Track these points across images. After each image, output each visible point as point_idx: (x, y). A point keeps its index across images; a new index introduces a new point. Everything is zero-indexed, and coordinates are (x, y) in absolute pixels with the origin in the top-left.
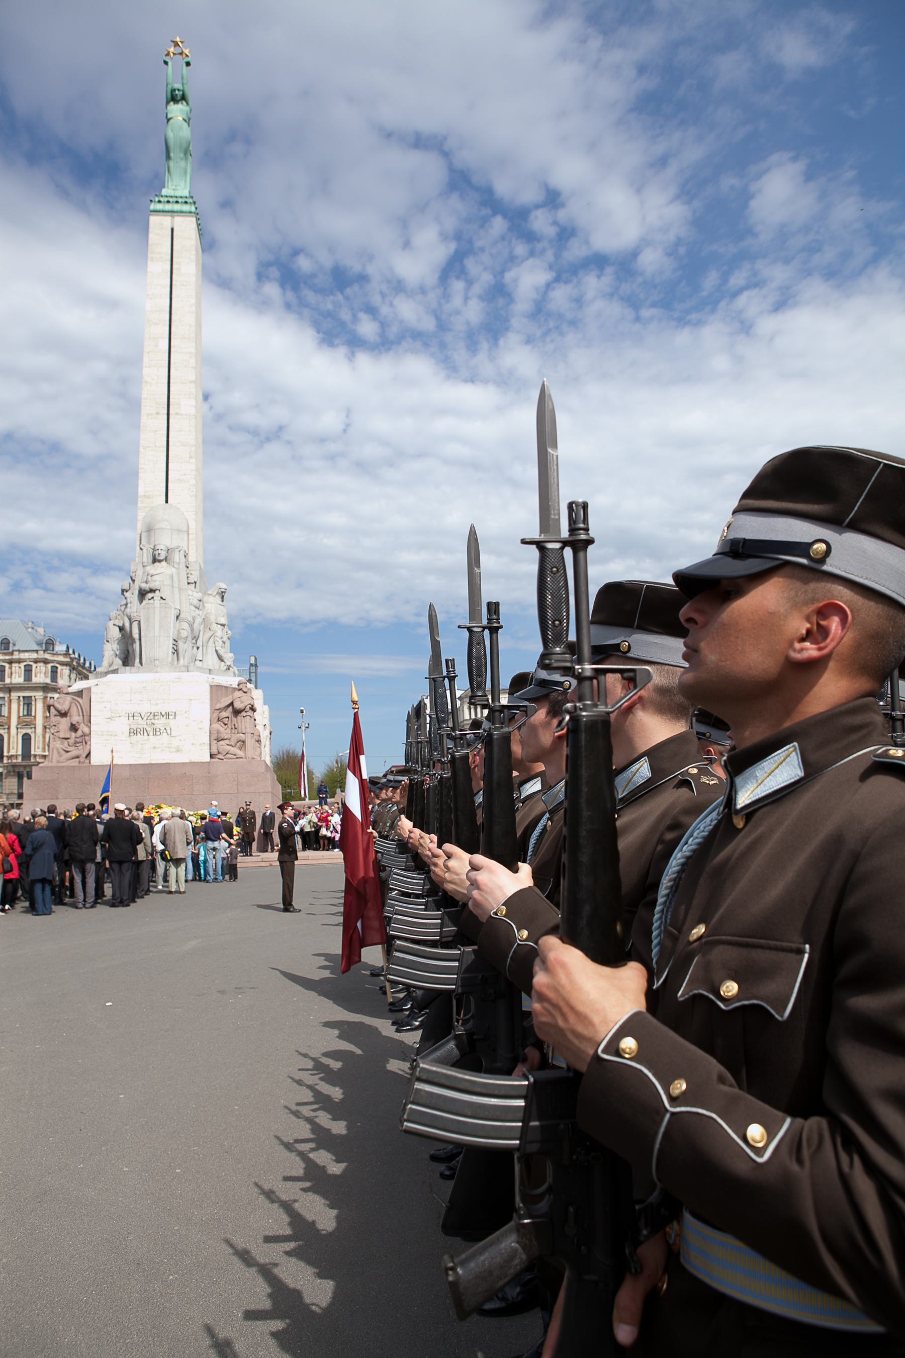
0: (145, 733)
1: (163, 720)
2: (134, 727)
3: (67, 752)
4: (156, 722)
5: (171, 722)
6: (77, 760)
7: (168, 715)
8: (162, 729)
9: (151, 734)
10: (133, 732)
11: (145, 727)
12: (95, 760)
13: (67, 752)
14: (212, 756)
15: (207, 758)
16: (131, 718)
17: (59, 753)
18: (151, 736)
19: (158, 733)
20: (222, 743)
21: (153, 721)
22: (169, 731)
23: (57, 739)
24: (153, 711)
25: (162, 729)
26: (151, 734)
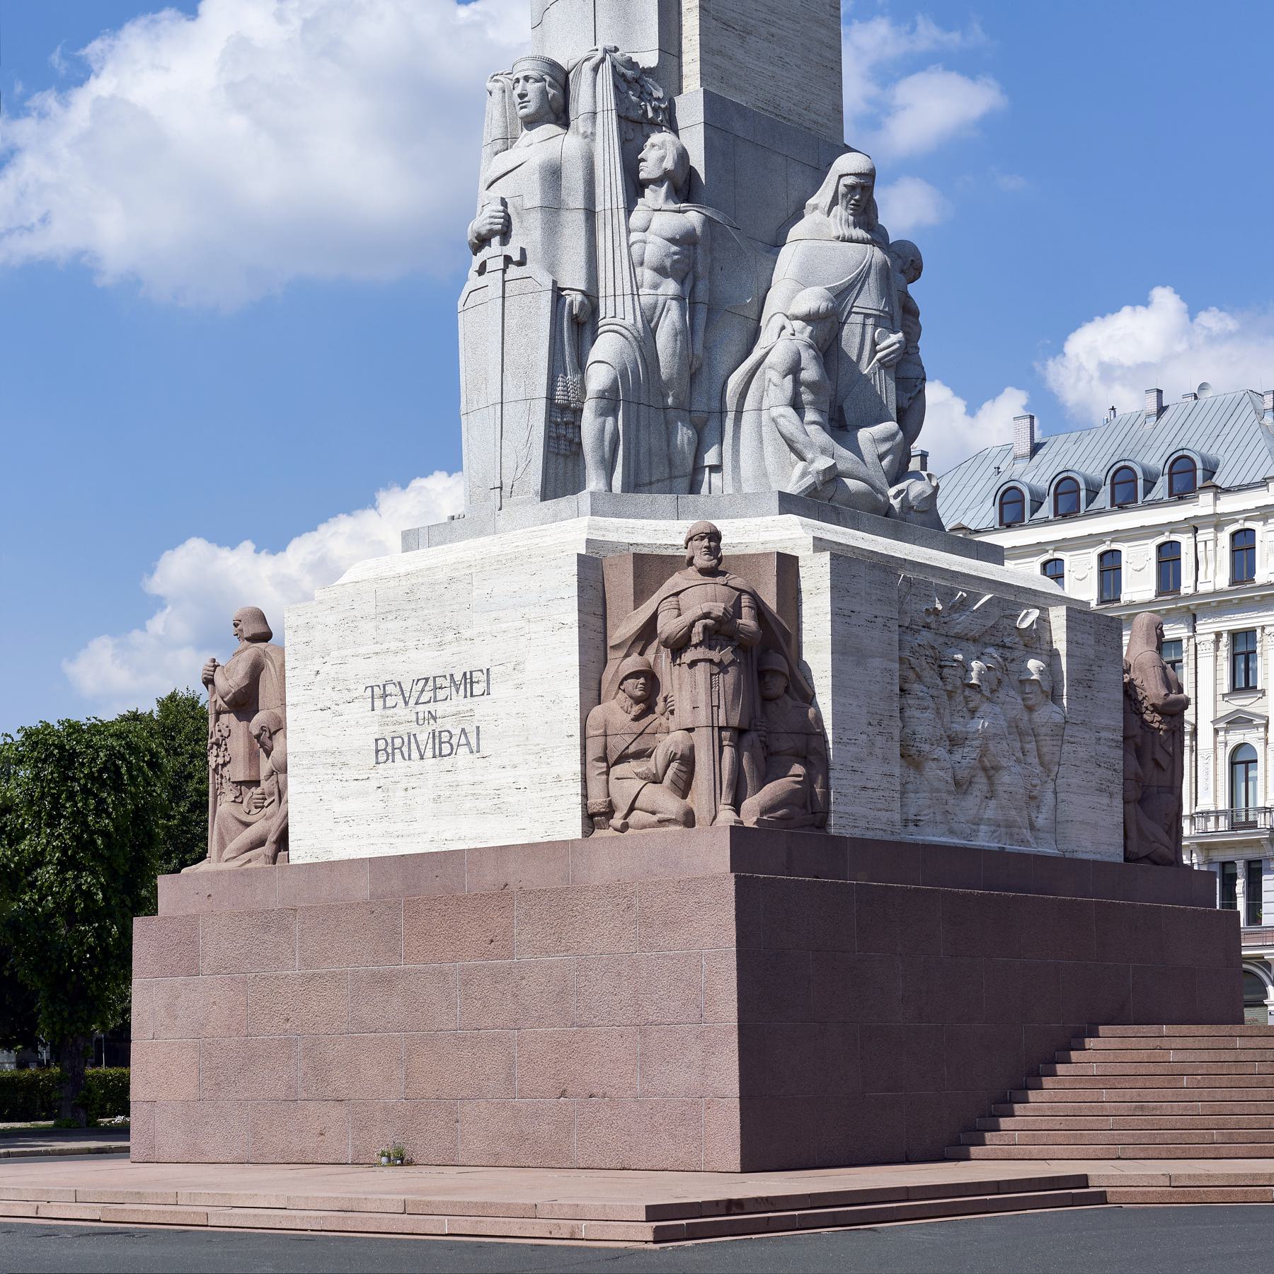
0: (415, 755)
1: (458, 702)
3: (247, 825)
4: (440, 708)
5: (482, 707)
7: (468, 679)
8: (456, 732)
9: (429, 753)
10: (386, 750)
11: (414, 729)
12: (299, 852)
13: (247, 825)
14: (592, 820)
16: (379, 703)
18: (429, 762)
19: (446, 749)
20: (618, 770)
22: (473, 741)
23: (227, 786)
25: (456, 732)
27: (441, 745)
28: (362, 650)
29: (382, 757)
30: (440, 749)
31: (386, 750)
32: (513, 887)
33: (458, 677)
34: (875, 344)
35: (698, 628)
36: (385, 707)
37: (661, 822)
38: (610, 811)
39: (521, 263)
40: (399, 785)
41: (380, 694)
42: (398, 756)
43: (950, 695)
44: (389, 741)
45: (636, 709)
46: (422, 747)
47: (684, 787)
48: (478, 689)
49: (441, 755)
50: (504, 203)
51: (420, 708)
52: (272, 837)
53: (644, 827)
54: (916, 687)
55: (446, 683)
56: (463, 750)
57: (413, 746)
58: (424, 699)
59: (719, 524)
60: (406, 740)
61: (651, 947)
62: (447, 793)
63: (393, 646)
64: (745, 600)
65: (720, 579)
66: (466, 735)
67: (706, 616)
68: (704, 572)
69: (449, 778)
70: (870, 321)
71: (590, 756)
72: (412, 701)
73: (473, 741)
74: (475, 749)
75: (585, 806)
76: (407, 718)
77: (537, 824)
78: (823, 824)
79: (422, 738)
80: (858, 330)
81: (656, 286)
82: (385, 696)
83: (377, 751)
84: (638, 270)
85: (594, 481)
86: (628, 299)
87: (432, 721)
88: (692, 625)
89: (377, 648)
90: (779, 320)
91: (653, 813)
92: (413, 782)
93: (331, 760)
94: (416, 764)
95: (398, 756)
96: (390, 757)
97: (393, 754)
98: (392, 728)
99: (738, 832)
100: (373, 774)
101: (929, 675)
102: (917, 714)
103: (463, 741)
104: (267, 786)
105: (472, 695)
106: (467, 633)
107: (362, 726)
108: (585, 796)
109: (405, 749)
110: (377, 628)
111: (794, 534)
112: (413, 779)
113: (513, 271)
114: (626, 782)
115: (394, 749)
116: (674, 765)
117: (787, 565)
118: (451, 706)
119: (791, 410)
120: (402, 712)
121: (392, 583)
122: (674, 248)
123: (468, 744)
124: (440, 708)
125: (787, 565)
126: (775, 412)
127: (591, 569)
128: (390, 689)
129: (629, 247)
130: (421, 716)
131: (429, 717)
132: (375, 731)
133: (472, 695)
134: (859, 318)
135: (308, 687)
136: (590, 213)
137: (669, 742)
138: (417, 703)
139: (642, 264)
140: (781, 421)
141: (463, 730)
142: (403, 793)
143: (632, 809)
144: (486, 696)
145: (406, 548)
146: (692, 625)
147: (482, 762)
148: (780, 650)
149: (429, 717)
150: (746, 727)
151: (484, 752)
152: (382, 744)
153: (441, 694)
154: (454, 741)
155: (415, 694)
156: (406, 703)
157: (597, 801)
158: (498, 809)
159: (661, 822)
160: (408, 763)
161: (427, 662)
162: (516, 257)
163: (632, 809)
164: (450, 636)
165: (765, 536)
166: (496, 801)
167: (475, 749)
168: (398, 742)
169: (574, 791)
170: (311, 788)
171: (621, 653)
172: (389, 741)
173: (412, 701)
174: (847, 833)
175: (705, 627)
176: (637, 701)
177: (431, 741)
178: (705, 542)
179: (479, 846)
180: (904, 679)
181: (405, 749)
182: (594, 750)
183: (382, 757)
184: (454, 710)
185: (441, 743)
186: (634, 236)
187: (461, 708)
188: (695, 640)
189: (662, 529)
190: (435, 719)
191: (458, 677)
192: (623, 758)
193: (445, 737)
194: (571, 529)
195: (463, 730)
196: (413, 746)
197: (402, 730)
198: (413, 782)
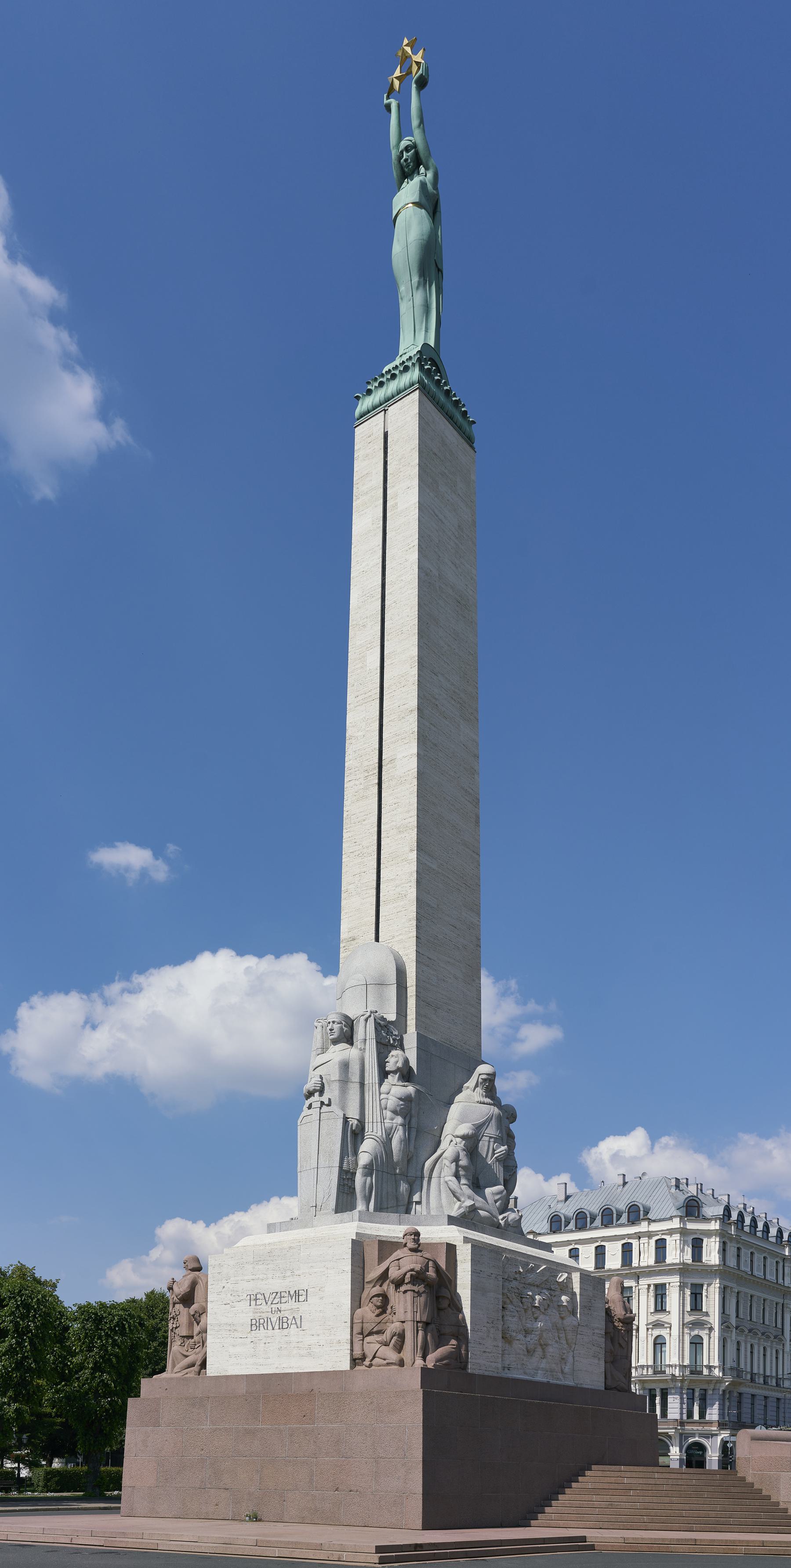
0: (270, 1327)
1: (292, 1304)
2: (257, 1316)
4: (283, 1307)
5: (303, 1307)
7: (297, 1294)
8: (290, 1317)
9: (277, 1327)
10: (256, 1325)
14: (355, 1361)
15: (345, 1365)
16: (253, 1303)
18: (277, 1331)
19: (285, 1325)
20: (368, 1339)
21: (279, 1306)
22: (299, 1323)
24: (279, 1290)
25: (290, 1317)
27: (283, 1324)
28: (246, 1278)
29: (254, 1328)
31: (256, 1325)
33: (292, 1293)
34: (494, 1150)
35: (408, 1275)
37: (388, 1364)
38: (364, 1358)
39: (329, 1105)
41: (254, 1298)
43: (526, 1310)
45: (378, 1311)
47: (399, 1348)
48: (301, 1298)
50: (321, 1077)
51: (273, 1306)
54: (510, 1307)
55: (286, 1295)
56: (294, 1326)
59: (420, 1229)
61: (382, 1422)
63: (261, 1277)
64: (431, 1264)
65: (419, 1254)
67: (412, 1270)
68: (411, 1250)
69: (286, 1339)
70: (492, 1140)
71: (355, 1332)
72: (269, 1303)
73: (299, 1323)
75: (352, 1355)
78: (465, 1368)
79: (274, 1320)
80: (487, 1144)
81: (392, 1119)
82: (256, 1299)
84: (384, 1111)
85: (360, 1206)
86: (379, 1124)
88: (405, 1274)
89: (253, 1277)
90: (450, 1137)
92: (269, 1340)
94: (270, 1332)
99: (425, 1370)
100: (249, 1335)
101: (516, 1301)
102: (510, 1319)
103: (294, 1322)
104: (197, 1338)
106: (297, 1273)
107: (244, 1313)
108: (352, 1350)
109: (265, 1325)
110: (254, 1268)
111: (454, 1234)
113: (324, 1108)
114: (372, 1345)
116: (395, 1338)
117: (451, 1249)
118: (288, 1306)
119: (454, 1179)
120: (264, 1307)
121: (262, 1248)
122: (401, 1103)
124: (283, 1307)
125: (451, 1249)
126: (447, 1179)
127: (358, 1246)
128: (259, 1296)
129: (380, 1101)
131: (276, 1311)
132: (251, 1315)
134: (487, 1139)
135: (219, 1294)
136: (362, 1084)
137: (393, 1327)
139: (386, 1109)
140: (450, 1183)
143: (374, 1357)
145: (269, 1232)
146: (405, 1274)
148: (446, 1287)
149: (276, 1311)
150: (429, 1321)
152: (254, 1322)
153: (283, 1300)
154: (289, 1322)
155: (271, 1299)
157: (358, 1353)
159: (388, 1364)
161: (277, 1284)
162: (326, 1102)
163: (374, 1357)
164: (289, 1273)
165: (441, 1235)
168: (262, 1321)
170: (218, 1341)
171: (371, 1285)
173: (269, 1303)
174: (476, 1372)
175: (411, 1275)
176: (378, 1307)
178: (413, 1237)
180: (504, 1303)
181: (265, 1325)
182: (357, 1329)
183: (254, 1328)
184: (290, 1308)
186: (383, 1096)
188: (406, 1281)
189: (393, 1229)
191: (292, 1293)
192: (370, 1334)
193: (285, 1320)
194: (349, 1227)
197: (264, 1315)
198: (269, 1340)
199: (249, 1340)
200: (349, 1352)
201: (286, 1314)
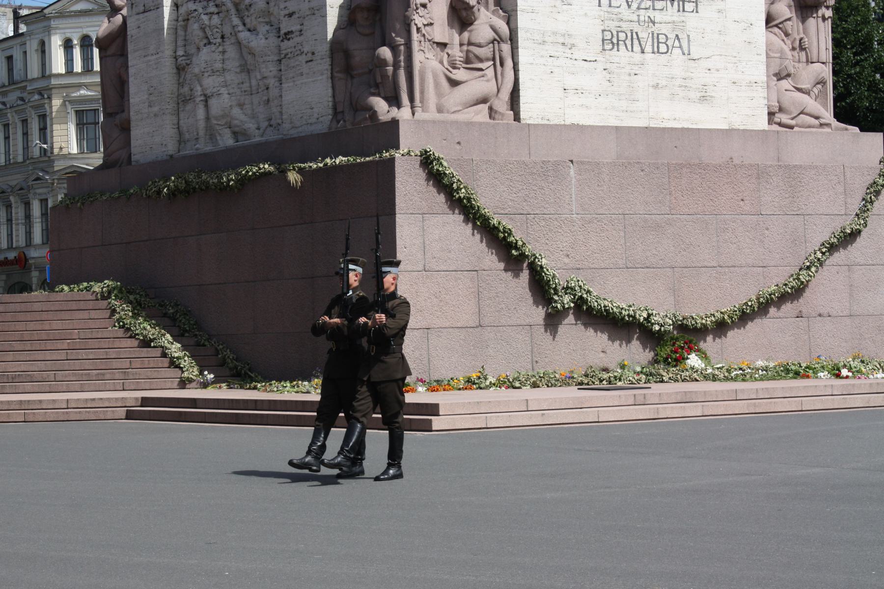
0: (637, 48)
2: (612, 25)
4: (658, 16)
6: (484, 107)
8: (672, 36)
9: (648, 49)
10: (612, 41)
11: (636, 28)
15: (762, 123)
17: (437, 85)
18: (649, 56)
19: (663, 48)
21: (651, 13)
26: (648, 49)
30: (658, 47)
31: (612, 41)
32: (736, 161)
36: (610, 6)
40: (623, 70)
42: (622, 47)
44: (615, 33)
46: (643, 44)
49: (658, 52)
51: (642, 12)
52: (505, 95)
53: (809, 127)
56: (677, 51)
57: (636, 42)
58: (643, 6)
60: (629, 35)
62: (664, 83)
66: (678, 39)
74: (686, 52)
76: (630, 18)
77: (735, 116)
83: (603, 40)
87: (651, 24)
91: (817, 118)
93: (561, 40)
94: (638, 56)
95: (622, 47)
96: (615, 45)
97: (618, 44)
98: (618, 24)
100: (600, 58)
103: (677, 44)
105: (684, 11)
112: (636, 68)
115: (618, 40)
123: (681, 47)
124: (658, 16)
130: (642, 18)
133: (684, 11)
138: (638, 8)
141: (677, 36)
142: (627, 78)
144: (694, 14)
147: (692, 63)
151: (694, 55)
152: (608, 36)
154: (670, 43)
156: (629, 6)
158: (703, 99)
159: (822, 125)
160: (631, 53)
166: (703, 94)
167: (686, 52)
168: (622, 36)
169: (762, 95)
172: (615, 33)
177: (650, 39)
179: (691, 126)
181: (628, 42)
185: (658, 43)
187: (675, 19)
190: (654, 23)
193: (662, 39)
195: (677, 36)
196: (636, 42)
197: (625, 26)
198: (636, 69)
199: (600, 66)
200: (766, 102)
201: (664, 29)
